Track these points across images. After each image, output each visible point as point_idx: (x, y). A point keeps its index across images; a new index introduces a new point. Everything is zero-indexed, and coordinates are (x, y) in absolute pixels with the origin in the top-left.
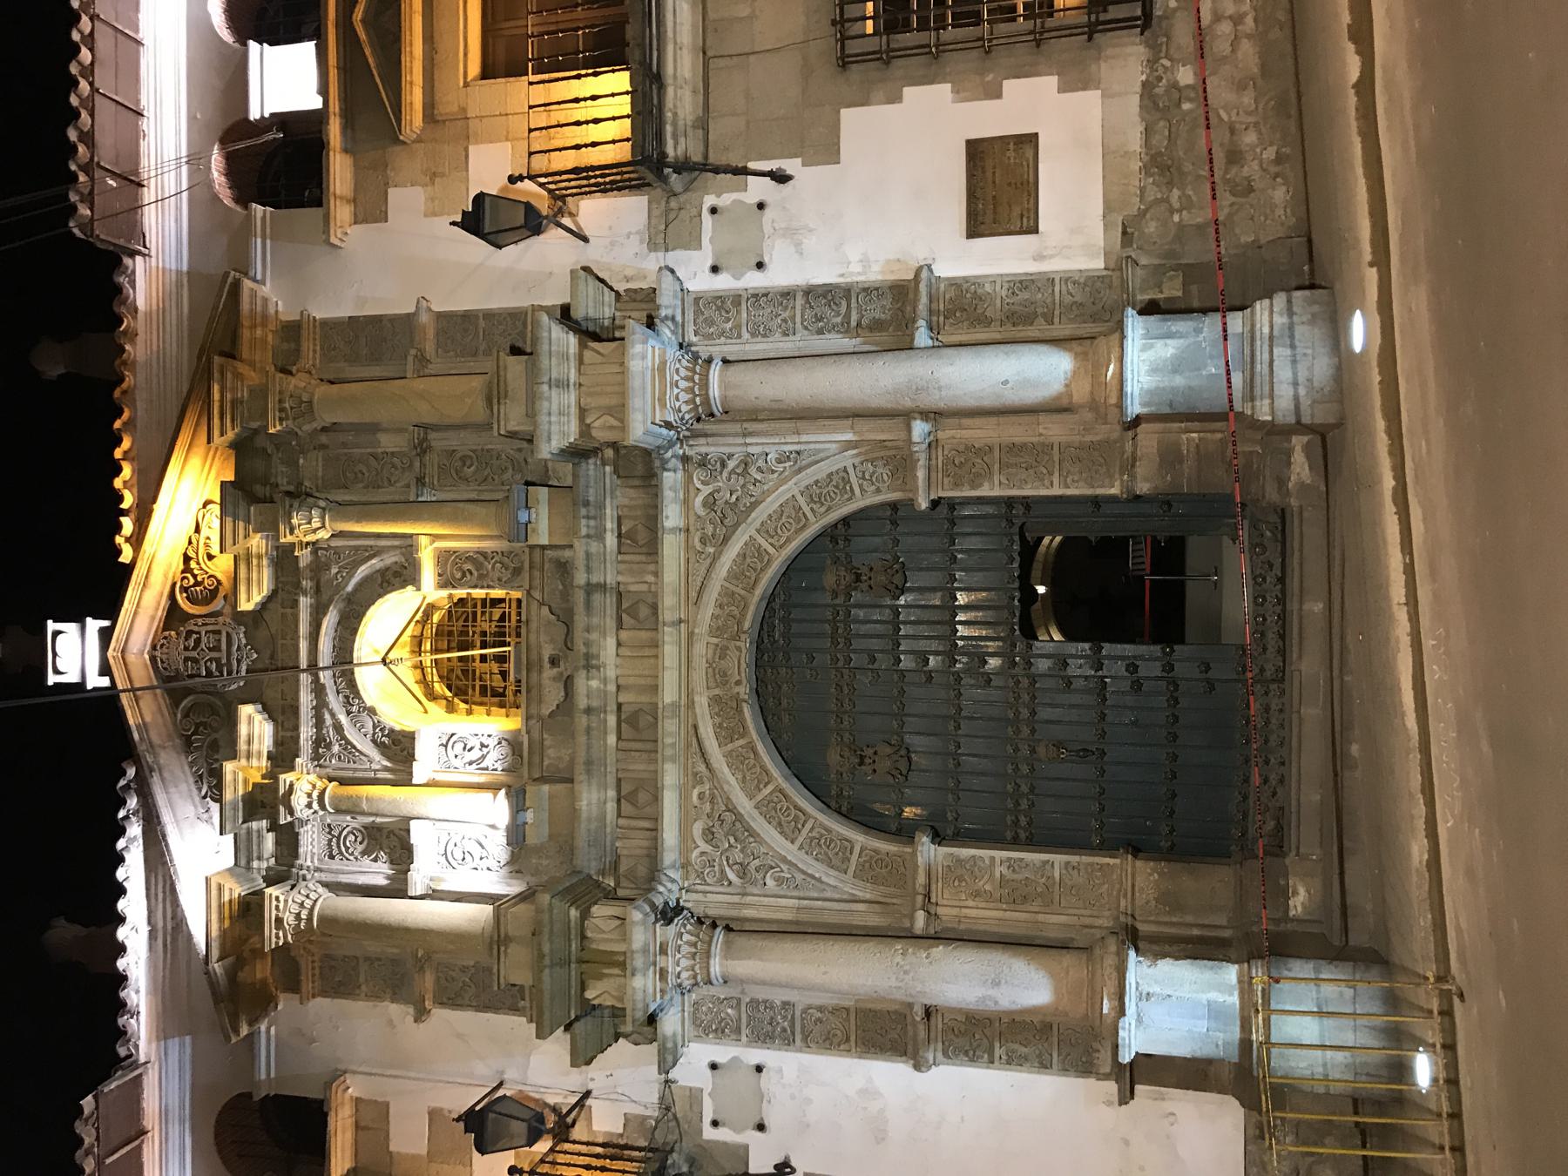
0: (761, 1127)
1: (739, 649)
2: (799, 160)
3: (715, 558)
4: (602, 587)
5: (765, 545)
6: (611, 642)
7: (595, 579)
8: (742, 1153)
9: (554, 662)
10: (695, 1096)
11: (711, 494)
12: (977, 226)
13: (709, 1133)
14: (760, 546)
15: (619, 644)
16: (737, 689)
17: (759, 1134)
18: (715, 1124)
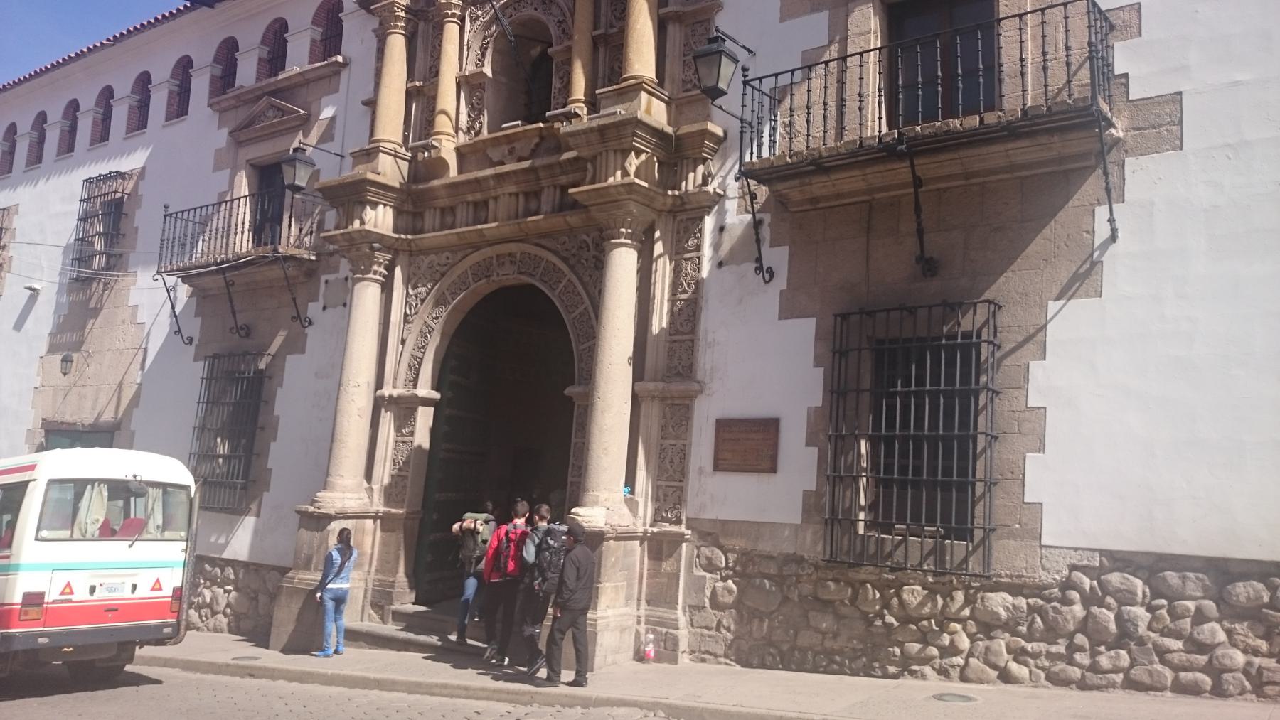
0: (324, 308)
1: (514, 273)
2: (785, 287)
3: (555, 253)
4: (538, 179)
5: (561, 286)
6: (513, 189)
7: (542, 174)
8: (314, 298)
9: (511, 152)
10: (336, 269)
11: (588, 246)
12: (723, 425)
13: (323, 278)
14: (561, 282)
15: (517, 195)
16: (495, 274)
17: (322, 308)
18: (327, 282)
